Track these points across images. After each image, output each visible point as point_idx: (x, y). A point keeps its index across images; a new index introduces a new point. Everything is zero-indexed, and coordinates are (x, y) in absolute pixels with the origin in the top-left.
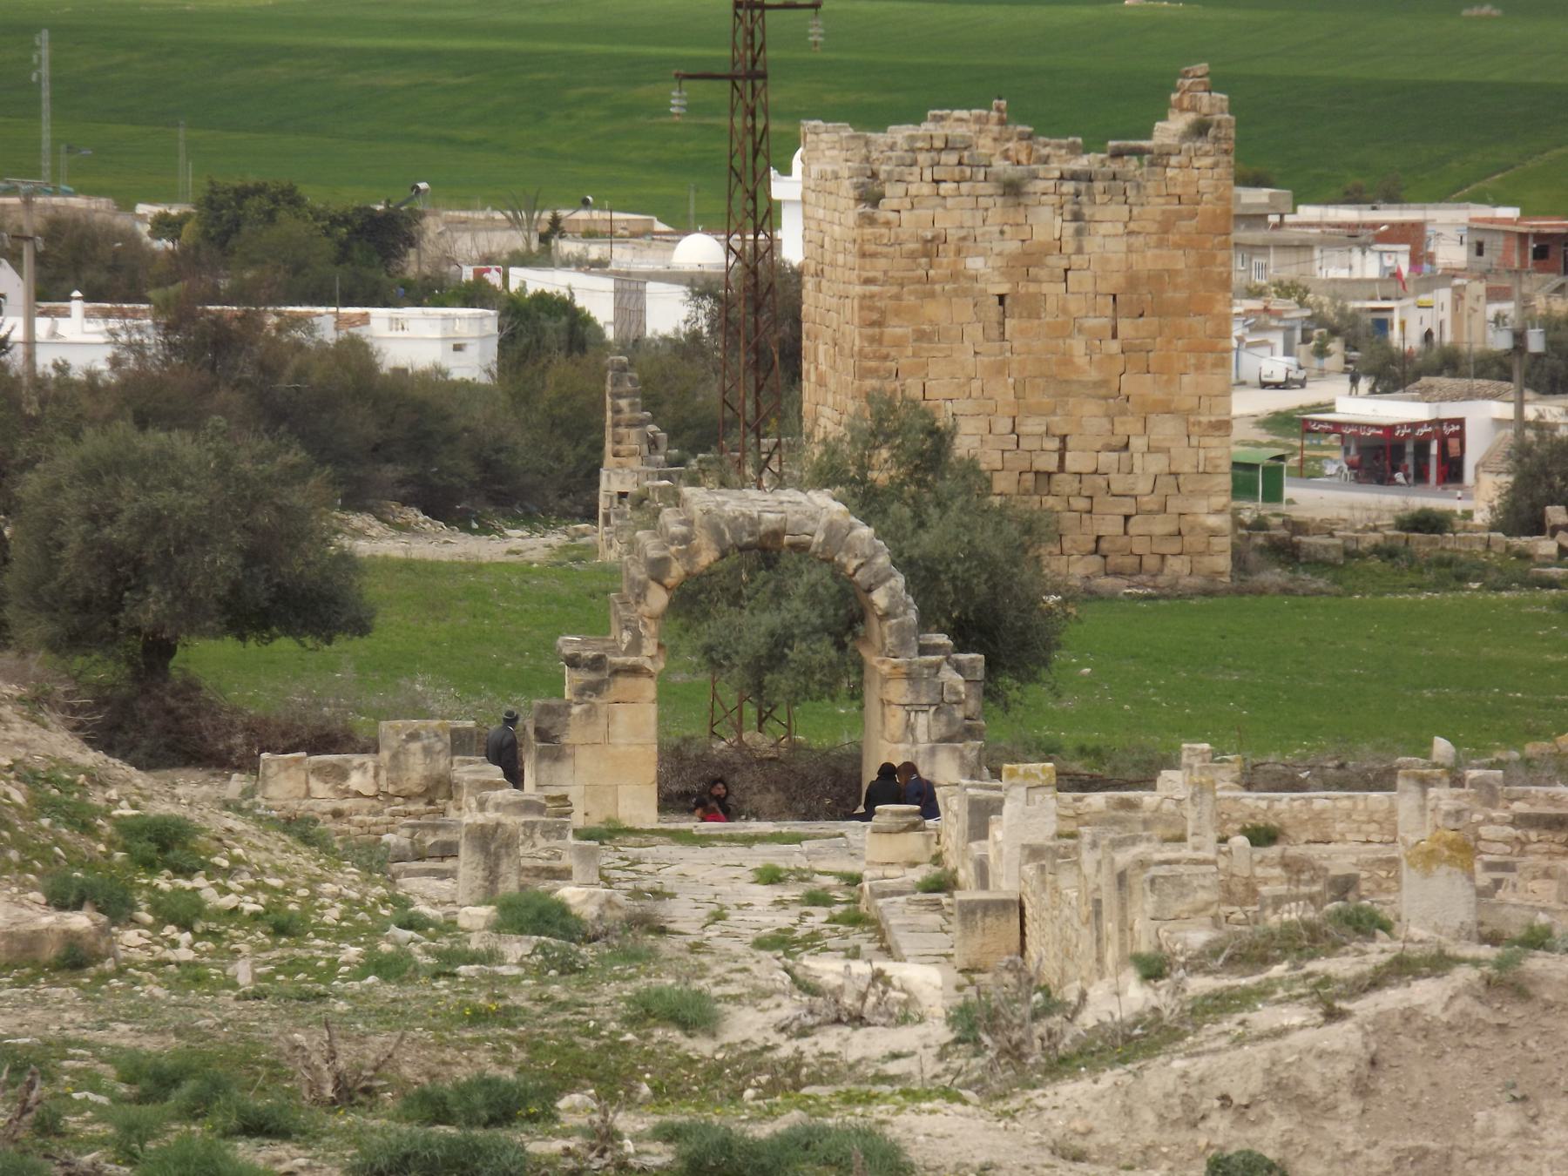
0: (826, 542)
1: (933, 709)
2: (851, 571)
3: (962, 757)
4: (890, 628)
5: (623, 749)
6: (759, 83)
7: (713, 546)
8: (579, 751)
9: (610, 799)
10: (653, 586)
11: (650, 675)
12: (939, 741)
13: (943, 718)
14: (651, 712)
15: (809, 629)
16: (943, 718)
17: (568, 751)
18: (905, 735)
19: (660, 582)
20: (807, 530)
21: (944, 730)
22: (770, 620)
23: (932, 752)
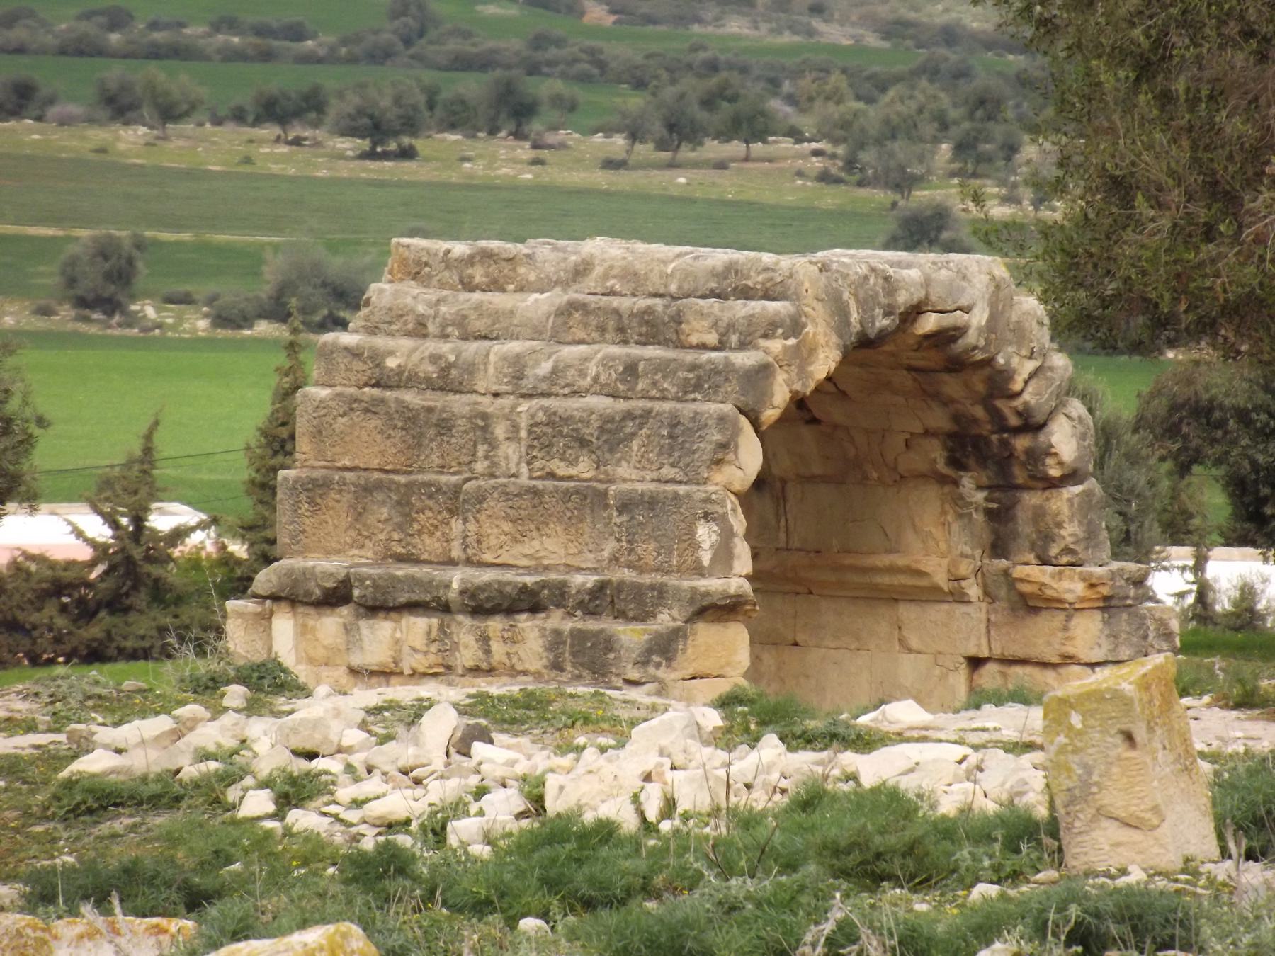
7: (834, 339)
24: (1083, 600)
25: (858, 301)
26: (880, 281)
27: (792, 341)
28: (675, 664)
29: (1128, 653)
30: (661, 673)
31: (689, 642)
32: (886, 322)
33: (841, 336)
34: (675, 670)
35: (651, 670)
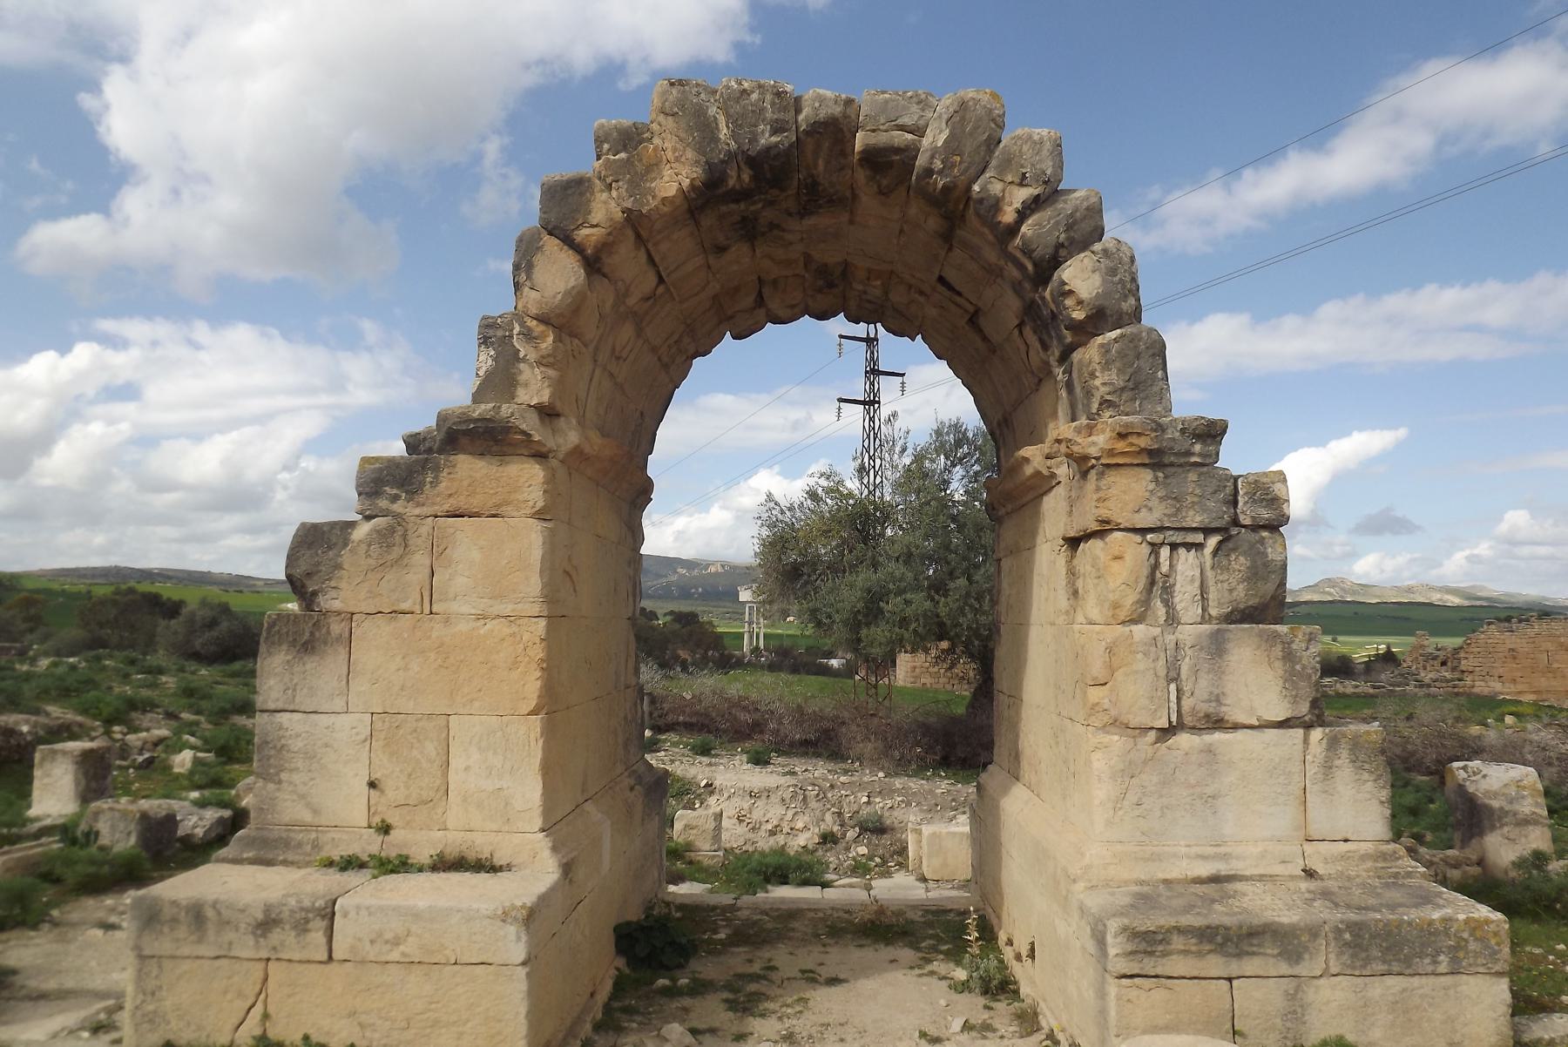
0: (953, 147)
1: (1213, 541)
2: (1008, 216)
3: (1289, 656)
4: (1105, 348)
5: (463, 627)
6: (876, 406)
7: (690, 154)
10: (551, 244)
11: (540, 456)
12: (1229, 618)
13: (1240, 563)
16: (1240, 563)
18: (1145, 602)
19: (568, 241)
20: (906, 120)
21: (1241, 591)
22: (864, 578)
23: (1216, 647)
24: (1111, 453)
25: (728, 116)
26: (769, 97)
27: (623, 155)
28: (421, 499)
29: (1198, 519)
30: (397, 507)
32: (774, 139)
33: (700, 150)
34: (418, 505)
35: (383, 503)
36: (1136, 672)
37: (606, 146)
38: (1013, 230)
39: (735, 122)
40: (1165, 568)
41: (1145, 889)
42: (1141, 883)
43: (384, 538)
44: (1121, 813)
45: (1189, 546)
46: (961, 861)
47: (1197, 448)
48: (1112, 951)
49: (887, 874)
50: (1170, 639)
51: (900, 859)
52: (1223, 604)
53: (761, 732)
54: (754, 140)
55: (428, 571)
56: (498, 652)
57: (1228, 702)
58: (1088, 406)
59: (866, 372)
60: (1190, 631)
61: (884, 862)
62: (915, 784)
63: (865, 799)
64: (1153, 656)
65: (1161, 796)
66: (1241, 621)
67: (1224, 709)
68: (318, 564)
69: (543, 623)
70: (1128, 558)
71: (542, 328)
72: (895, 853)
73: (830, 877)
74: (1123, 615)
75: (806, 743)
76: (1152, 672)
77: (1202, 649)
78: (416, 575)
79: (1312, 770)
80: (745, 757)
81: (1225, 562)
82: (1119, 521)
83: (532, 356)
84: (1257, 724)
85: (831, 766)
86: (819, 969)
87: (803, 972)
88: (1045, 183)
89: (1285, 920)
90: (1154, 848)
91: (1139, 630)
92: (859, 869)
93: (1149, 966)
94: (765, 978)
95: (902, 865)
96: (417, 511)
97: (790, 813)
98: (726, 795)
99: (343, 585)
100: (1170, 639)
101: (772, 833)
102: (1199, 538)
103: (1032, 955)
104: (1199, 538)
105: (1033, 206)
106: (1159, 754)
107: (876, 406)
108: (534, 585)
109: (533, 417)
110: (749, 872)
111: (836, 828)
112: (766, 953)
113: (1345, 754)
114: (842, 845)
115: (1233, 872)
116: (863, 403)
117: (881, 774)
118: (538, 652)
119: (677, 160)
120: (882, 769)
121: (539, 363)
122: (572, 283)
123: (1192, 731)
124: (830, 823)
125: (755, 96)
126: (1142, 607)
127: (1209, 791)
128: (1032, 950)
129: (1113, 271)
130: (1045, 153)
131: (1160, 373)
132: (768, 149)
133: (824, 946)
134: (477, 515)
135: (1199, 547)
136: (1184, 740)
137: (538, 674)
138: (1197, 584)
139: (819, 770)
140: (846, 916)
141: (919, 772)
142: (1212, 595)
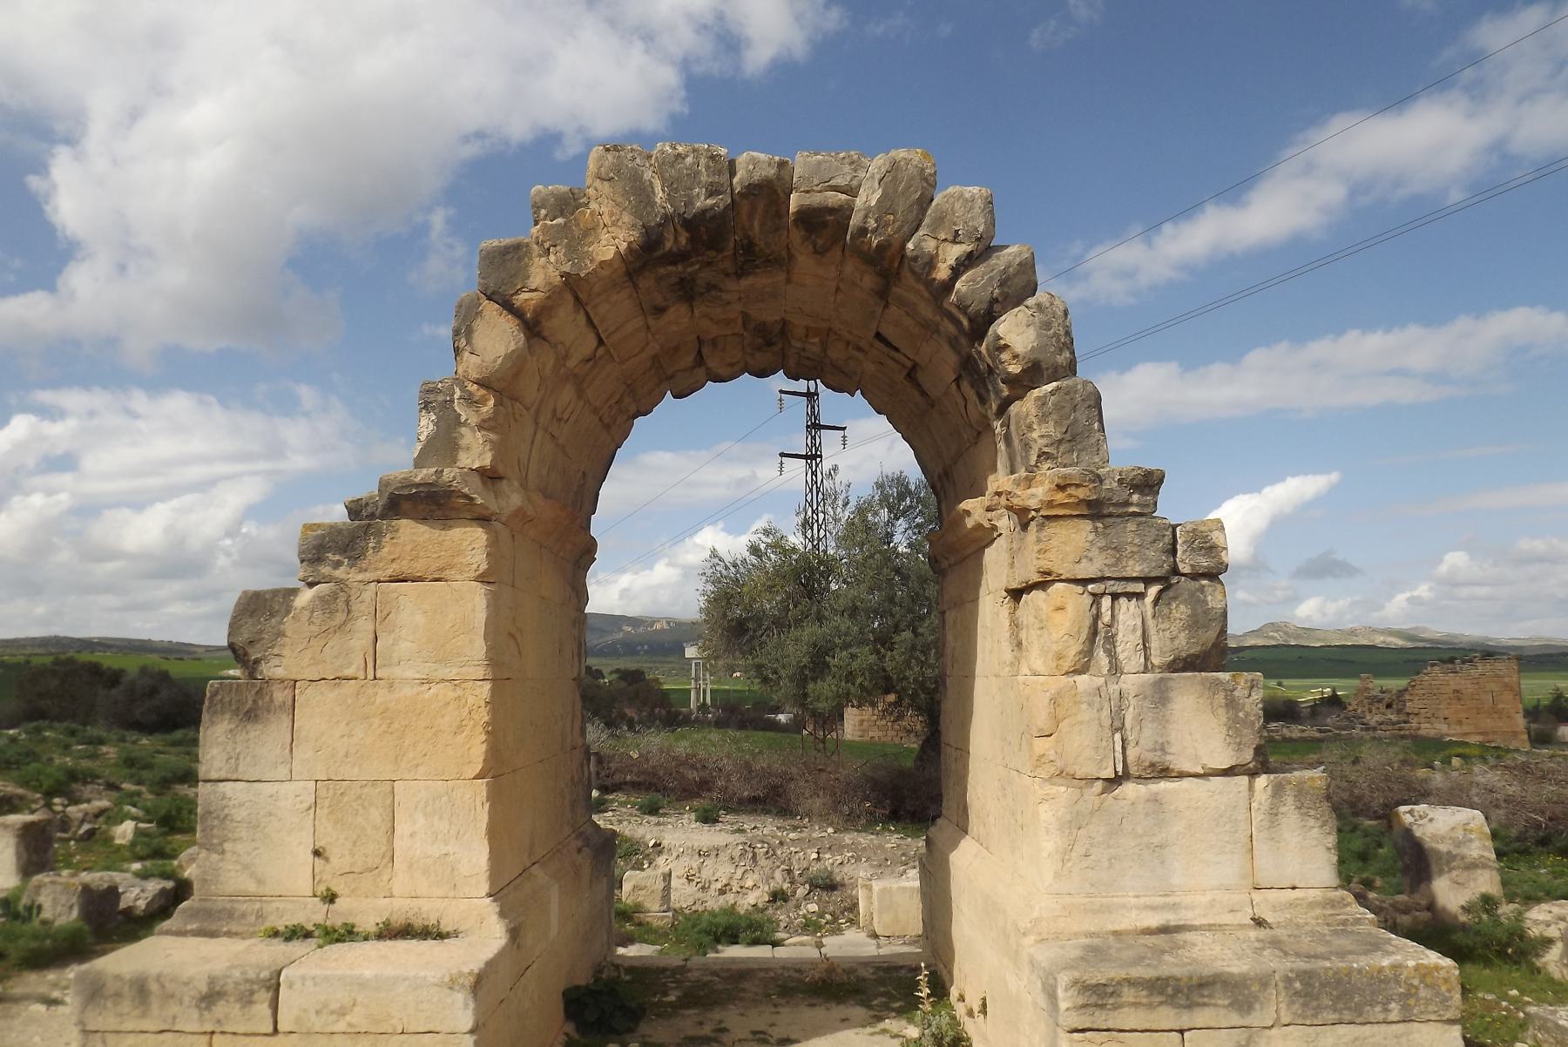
1: (1154, 590)
2: (942, 273)
3: (1232, 704)
4: (1042, 402)
5: (407, 691)
6: (819, 460)
8: (308, 698)
9: (376, 815)
10: (491, 309)
11: (483, 519)
13: (1181, 611)
14: (473, 603)
15: (849, 639)
16: (1181, 611)
17: (280, 695)
18: (1088, 652)
19: (508, 306)
23: (1160, 696)
24: (1050, 504)
25: (663, 180)
26: (703, 161)
27: (560, 220)
29: (1138, 568)
30: (340, 573)
31: (387, 538)
32: (710, 202)
33: (636, 214)
35: (325, 570)
36: (1082, 723)
37: (543, 212)
38: (948, 286)
39: (669, 185)
40: (1106, 618)
41: (1096, 941)
42: (1091, 935)
43: (326, 603)
44: (1069, 864)
45: (1130, 596)
46: (911, 917)
47: (1135, 497)
48: (1063, 1005)
49: (838, 931)
50: (1113, 688)
51: (851, 916)
52: (1166, 653)
53: (709, 790)
54: (689, 203)
55: (372, 636)
56: (443, 716)
57: (1172, 750)
58: (1026, 458)
59: (808, 427)
60: (1133, 682)
61: (835, 919)
62: (865, 839)
63: (815, 856)
64: (1097, 706)
65: (1109, 847)
66: (1184, 670)
67: (1168, 758)
68: (261, 631)
69: (487, 686)
70: (1070, 608)
71: (483, 392)
72: (846, 909)
73: (780, 935)
74: (1067, 665)
75: (754, 800)
76: (1097, 722)
77: (1145, 698)
78: (359, 641)
79: (1257, 817)
80: (693, 816)
81: (1166, 611)
82: (1061, 572)
83: (474, 420)
84: (1202, 772)
85: (780, 822)
86: (770, 1030)
87: (754, 1033)
88: (978, 239)
89: (1234, 970)
90: (1104, 900)
91: (1083, 680)
92: (810, 926)
93: (1100, 1019)
94: (716, 1040)
95: (853, 922)
96: (360, 577)
97: (740, 872)
98: (675, 855)
99: (285, 652)
100: (1113, 688)
101: (722, 892)
102: (1140, 587)
103: (984, 1009)
104: (1140, 587)
105: (966, 262)
106: (1106, 804)
107: (819, 460)
108: (478, 648)
109: (476, 480)
110: (699, 932)
111: (786, 886)
112: (717, 1015)
113: (1290, 800)
114: (791, 903)
115: (1182, 923)
116: (805, 457)
117: (830, 830)
118: (484, 716)
119: (614, 224)
120: (831, 825)
121: (480, 427)
122: (512, 347)
123: (1138, 780)
124: (779, 881)
125: (689, 160)
126: (1085, 657)
127: (1156, 840)
128: (984, 1005)
129: (1047, 325)
130: (977, 210)
131: (1096, 425)
132: (704, 212)
133: (775, 1006)
134: (420, 579)
135: (1140, 596)
136: (1130, 789)
137: (484, 737)
138: (1139, 633)
139: (768, 827)
140: (796, 975)
141: (868, 827)
142: (1154, 644)
